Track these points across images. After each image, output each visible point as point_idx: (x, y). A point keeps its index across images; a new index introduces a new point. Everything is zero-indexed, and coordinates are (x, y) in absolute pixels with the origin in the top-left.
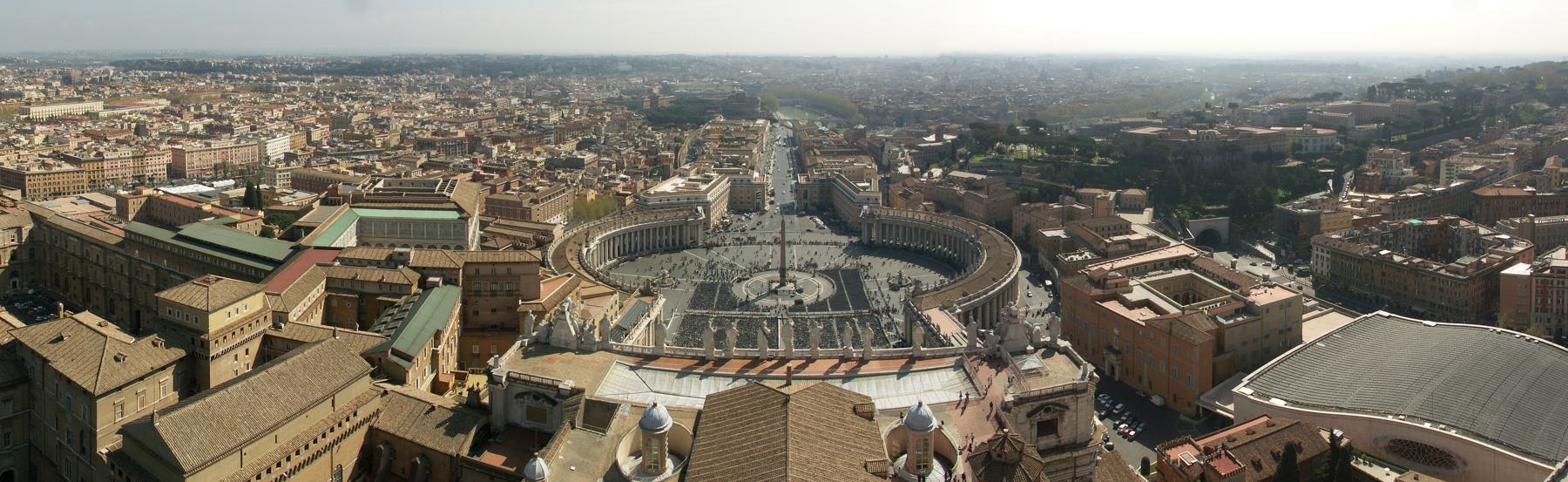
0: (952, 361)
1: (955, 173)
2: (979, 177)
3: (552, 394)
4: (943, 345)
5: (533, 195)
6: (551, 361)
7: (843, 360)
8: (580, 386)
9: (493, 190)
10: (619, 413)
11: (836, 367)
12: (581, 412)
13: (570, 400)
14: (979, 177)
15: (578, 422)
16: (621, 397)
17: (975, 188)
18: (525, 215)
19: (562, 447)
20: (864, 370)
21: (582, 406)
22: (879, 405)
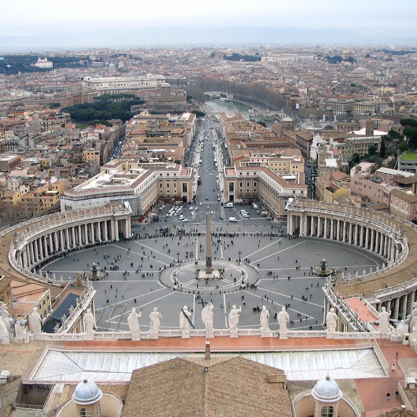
1: (382, 170)
4: (360, 331)
8: (16, 374)
10: (54, 391)
14: (407, 174)
16: (54, 379)
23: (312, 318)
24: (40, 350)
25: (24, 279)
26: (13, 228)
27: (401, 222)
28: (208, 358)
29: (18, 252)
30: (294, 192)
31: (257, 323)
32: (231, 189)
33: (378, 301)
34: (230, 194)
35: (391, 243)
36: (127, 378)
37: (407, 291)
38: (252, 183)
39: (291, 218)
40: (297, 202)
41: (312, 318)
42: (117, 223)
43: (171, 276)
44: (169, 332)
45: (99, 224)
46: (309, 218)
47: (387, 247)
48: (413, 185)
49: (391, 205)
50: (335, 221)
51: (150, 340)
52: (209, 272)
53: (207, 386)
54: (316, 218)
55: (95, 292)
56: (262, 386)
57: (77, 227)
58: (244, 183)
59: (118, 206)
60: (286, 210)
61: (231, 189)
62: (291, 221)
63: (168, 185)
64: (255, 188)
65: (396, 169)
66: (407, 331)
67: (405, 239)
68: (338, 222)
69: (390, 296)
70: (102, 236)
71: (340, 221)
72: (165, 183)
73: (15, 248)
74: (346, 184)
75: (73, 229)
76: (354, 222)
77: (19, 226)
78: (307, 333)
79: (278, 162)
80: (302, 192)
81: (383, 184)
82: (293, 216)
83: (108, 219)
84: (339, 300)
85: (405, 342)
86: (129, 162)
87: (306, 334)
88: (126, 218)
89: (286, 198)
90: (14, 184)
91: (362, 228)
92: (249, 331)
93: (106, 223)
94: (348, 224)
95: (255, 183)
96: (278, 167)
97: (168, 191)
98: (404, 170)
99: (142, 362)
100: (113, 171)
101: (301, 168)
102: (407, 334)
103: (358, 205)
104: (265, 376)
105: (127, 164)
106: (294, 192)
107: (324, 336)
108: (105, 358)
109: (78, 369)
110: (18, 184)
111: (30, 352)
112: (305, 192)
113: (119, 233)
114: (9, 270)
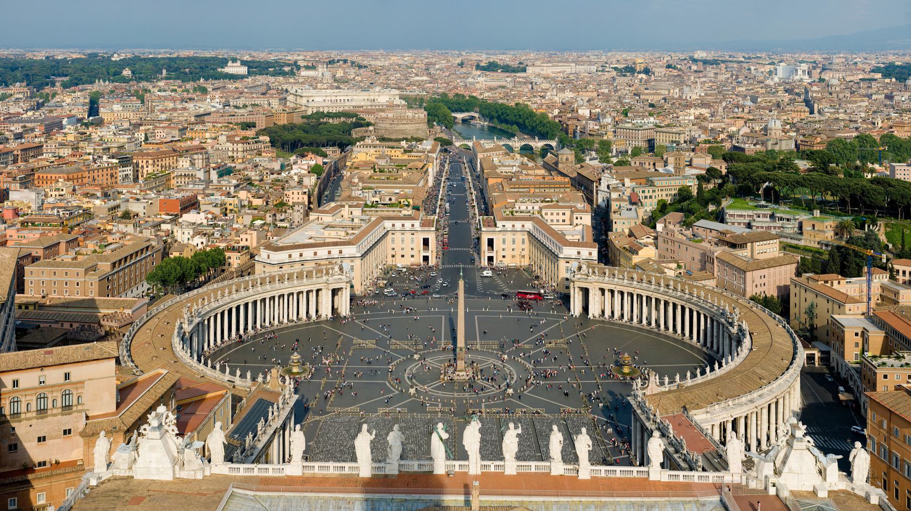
2: (741, 230)
17: (733, 246)
24: (220, 491)
30: (579, 253)
31: (543, 455)
34: (488, 254)
39: (577, 290)
40: (584, 267)
42: (330, 292)
44: (414, 466)
46: (602, 291)
48: (749, 245)
50: (640, 297)
51: (386, 476)
57: (274, 297)
59: (333, 269)
66: (772, 473)
67: (745, 326)
68: (644, 299)
70: (307, 312)
71: (647, 297)
74: (651, 244)
75: (267, 301)
76: (667, 298)
78: (619, 471)
79: (555, 211)
80: (590, 254)
81: (703, 244)
83: (318, 287)
85: (772, 491)
86: (350, 206)
87: (618, 472)
88: (343, 285)
89: (568, 260)
90: (186, 233)
91: (679, 307)
92: (533, 466)
94: (656, 299)
96: (555, 217)
97: (402, 249)
100: (327, 219)
101: (587, 219)
102: (773, 479)
103: (671, 274)
105: (347, 207)
106: (579, 253)
107: (646, 476)
108: (319, 506)
110: (191, 233)
111: (205, 495)
112: (595, 253)
113: (333, 307)
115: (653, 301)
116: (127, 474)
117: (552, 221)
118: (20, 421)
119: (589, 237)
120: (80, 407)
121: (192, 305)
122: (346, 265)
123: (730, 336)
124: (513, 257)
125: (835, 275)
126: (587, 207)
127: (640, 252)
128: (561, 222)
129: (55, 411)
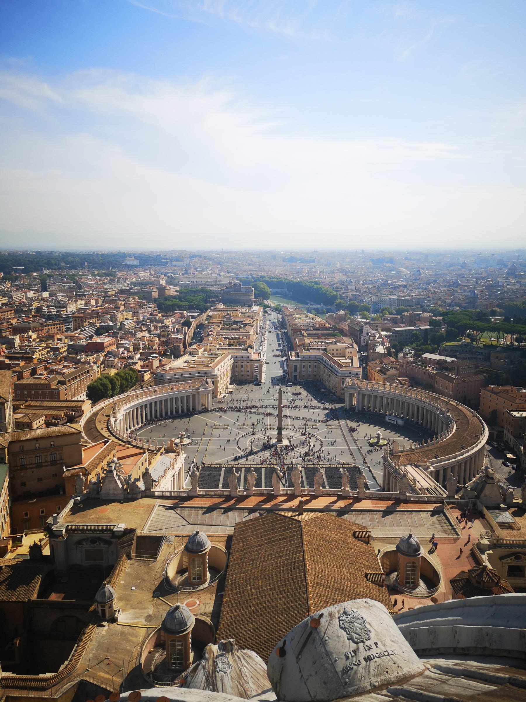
0: (431, 507)
1: (427, 355)
3: (106, 536)
5: (60, 378)
6: (102, 512)
7: (340, 497)
8: (131, 527)
9: (20, 376)
11: (334, 502)
12: (134, 547)
13: (125, 538)
14: (449, 359)
15: (133, 554)
17: (446, 369)
18: (54, 395)
19: (122, 575)
20: (357, 506)
21: (134, 542)
22: (374, 533)
23: (372, 483)
24: (151, 505)
25: (124, 444)
26: (111, 400)
27: (447, 400)
28: (300, 514)
29: (116, 421)
32: (296, 370)
33: (432, 469)
34: (294, 374)
35: (438, 419)
36: (230, 531)
37: (458, 461)
38: (312, 365)
39: (348, 395)
41: (372, 483)
43: (247, 443)
45: (185, 398)
47: (435, 422)
49: (436, 385)
52: (280, 440)
53: (305, 538)
54: (370, 396)
55: (185, 455)
56: (351, 540)
57: (167, 399)
58: (306, 365)
60: (343, 389)
61: (296, 370)
62: (348, 398)
63: (242, 366)
64: (315, 369)
65: (439, 354)
68: (389, 400)
69: (443, 466)
72: (239, 364)
73: (114, 417)
77: (116, 398)
81: (427, 368)
82: (350, 394)
84: (397, 467)
93: (191, 397)
94: (398, 401)
95: (315, 366)
96: (335, 352)
98: (447, 356)
99: (240, 516)
104: (352, 532)
109: (185, 523)
114: (109, 436)
115: (395, 401)
116: (96, 497)
117: (333, 354)
118: (26, 469)
119: (356, 362)
120: (61, 462)
121: (119, 405)
122: (209, 381)
123: (442, 423)
124: (310, 376)
125: (508, 388)
126: (356, 346)
127: (387, 373)
128: (338, 354)
129: (46, 464)
